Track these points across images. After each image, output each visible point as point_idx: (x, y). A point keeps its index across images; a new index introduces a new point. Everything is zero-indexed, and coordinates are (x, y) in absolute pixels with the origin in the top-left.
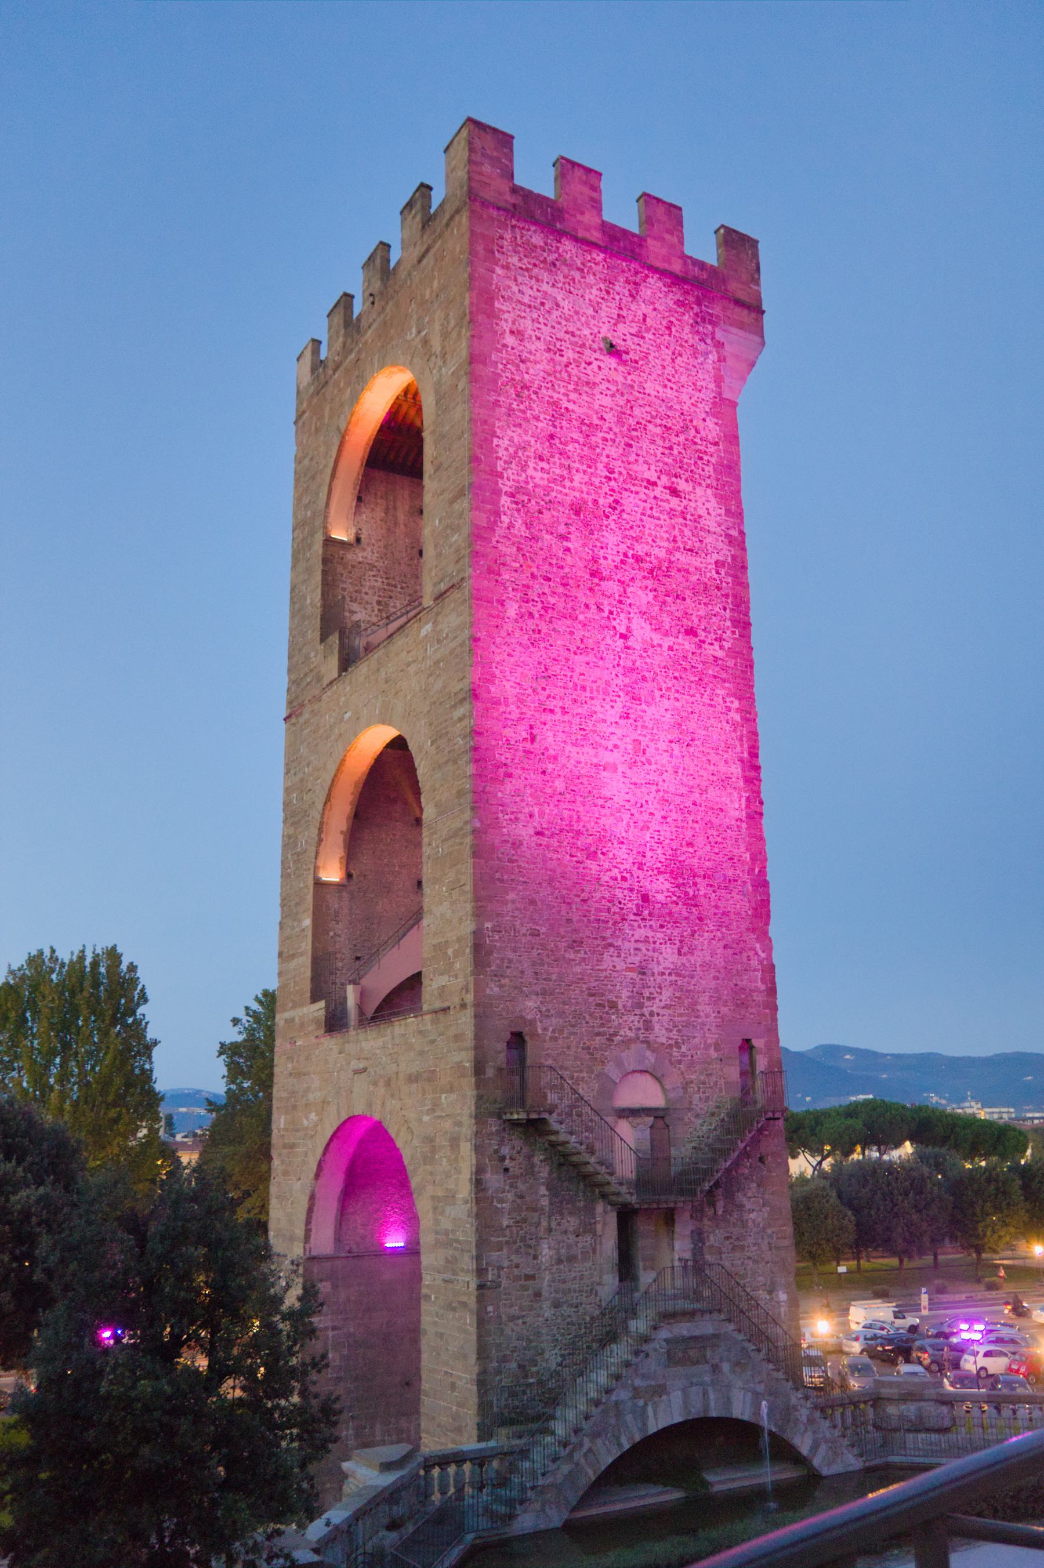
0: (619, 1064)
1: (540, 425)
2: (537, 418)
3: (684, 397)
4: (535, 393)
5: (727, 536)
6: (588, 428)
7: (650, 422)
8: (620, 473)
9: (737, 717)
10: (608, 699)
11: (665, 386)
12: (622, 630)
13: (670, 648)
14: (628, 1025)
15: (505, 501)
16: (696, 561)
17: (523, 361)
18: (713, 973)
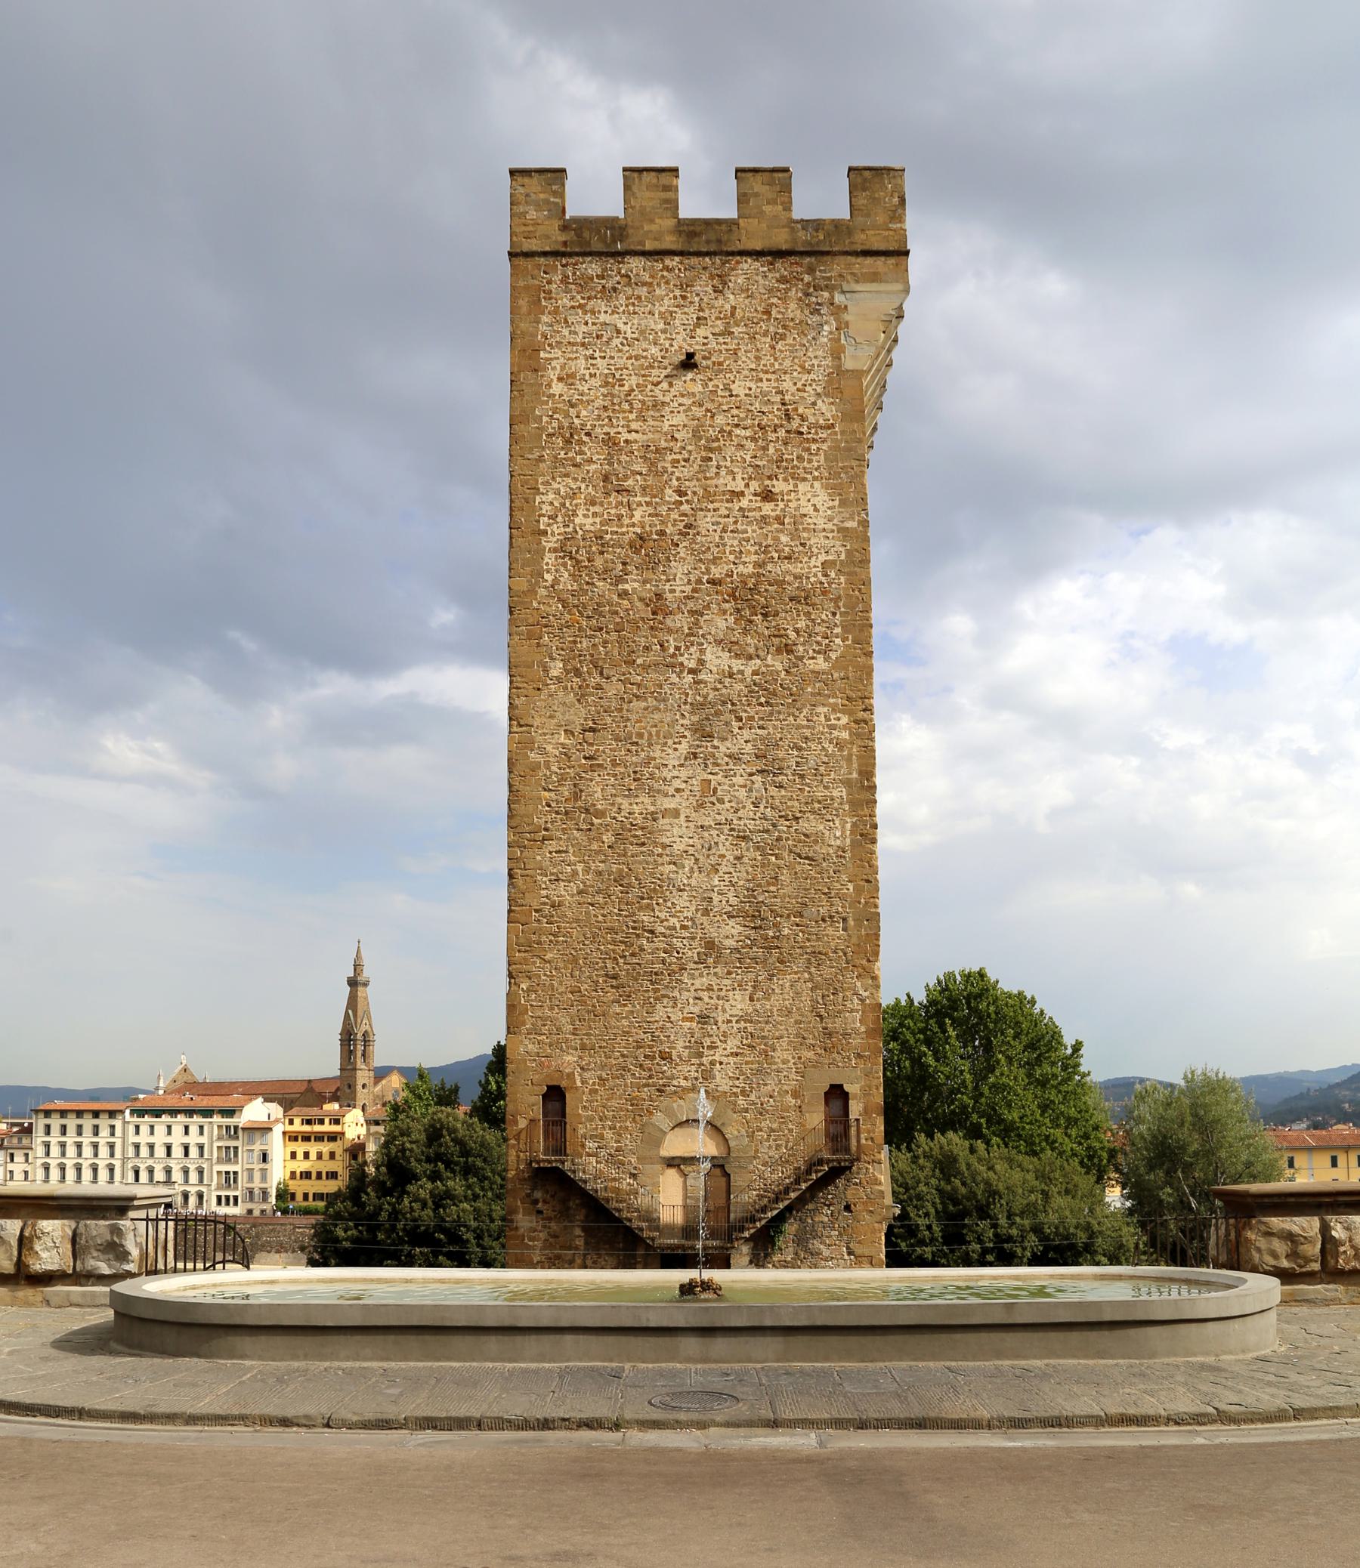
0: (669, 1113)
1: (593, 467)
2: (590, 461)
3: (787, 384)
4: (588, 434)
5: (840, 530)
6: (652, 454)
7: (737, 426)
8: (695, 493)
9: (845, 735)
10: (670, 742)
11: (761, 380)
12: (692, 664)
13: (755, 673)
14: (684, 1073)
15: (549, 558)
16: (796, 568)
17: (572, 406)
18: (796, 1016)
